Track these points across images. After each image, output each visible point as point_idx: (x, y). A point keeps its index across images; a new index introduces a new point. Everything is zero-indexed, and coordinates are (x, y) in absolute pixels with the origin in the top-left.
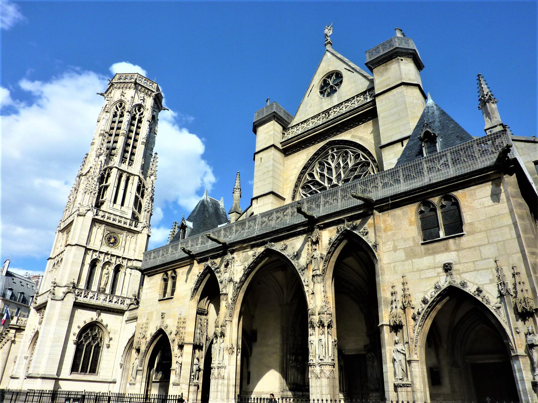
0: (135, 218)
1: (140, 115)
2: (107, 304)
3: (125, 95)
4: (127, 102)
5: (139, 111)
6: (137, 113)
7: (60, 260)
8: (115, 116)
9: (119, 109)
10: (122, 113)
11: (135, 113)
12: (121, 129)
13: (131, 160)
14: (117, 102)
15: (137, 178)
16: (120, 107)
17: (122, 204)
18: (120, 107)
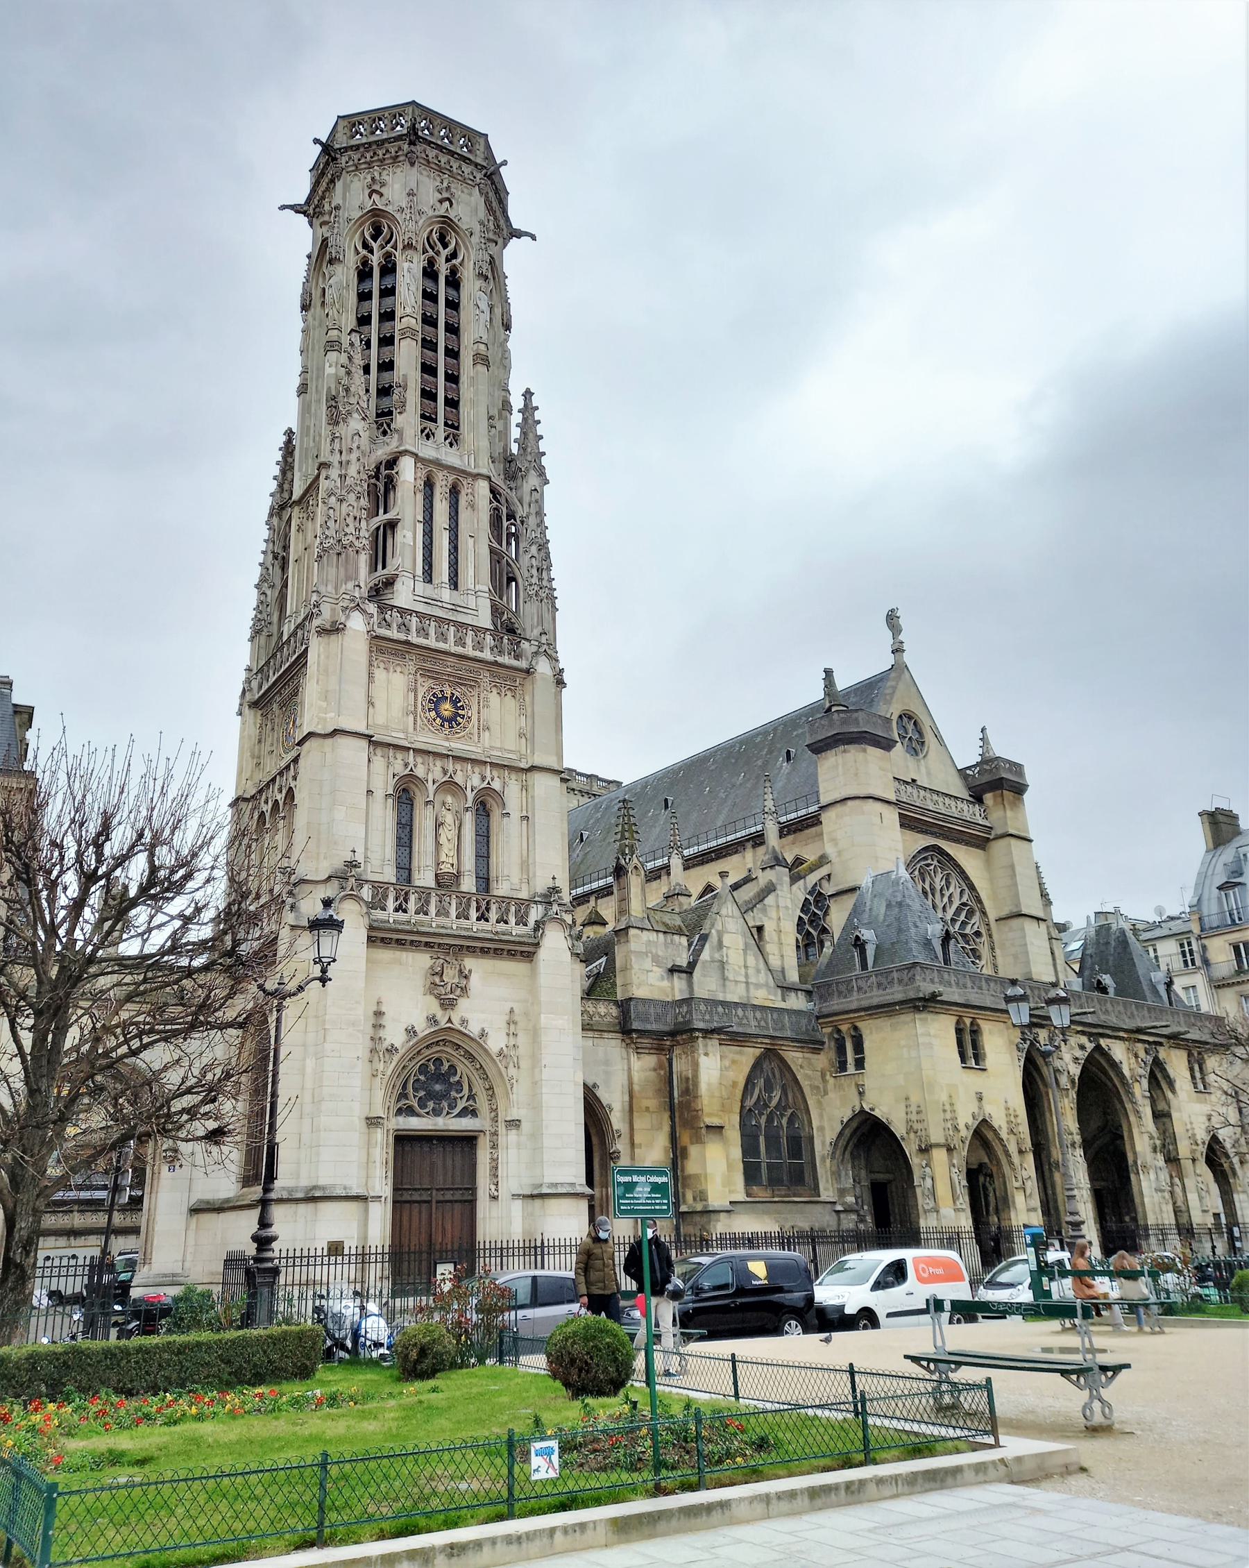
0: (507, 629)
1: (447, 260)
2: (473, 925)
3: (382, 190)
4: (397, 216)
5: (445, 246)
6: (438, 253)
7: (280, 797)
8: (364, 273)
9: (375, 246)
10: (388, 256)
11: (431, 253)
12: (398, 315)
13: (453, 426)
14: (360, 222)
15: (483, 488)
16: (375, 238)
17: (454, 583)
18: (375, 238)
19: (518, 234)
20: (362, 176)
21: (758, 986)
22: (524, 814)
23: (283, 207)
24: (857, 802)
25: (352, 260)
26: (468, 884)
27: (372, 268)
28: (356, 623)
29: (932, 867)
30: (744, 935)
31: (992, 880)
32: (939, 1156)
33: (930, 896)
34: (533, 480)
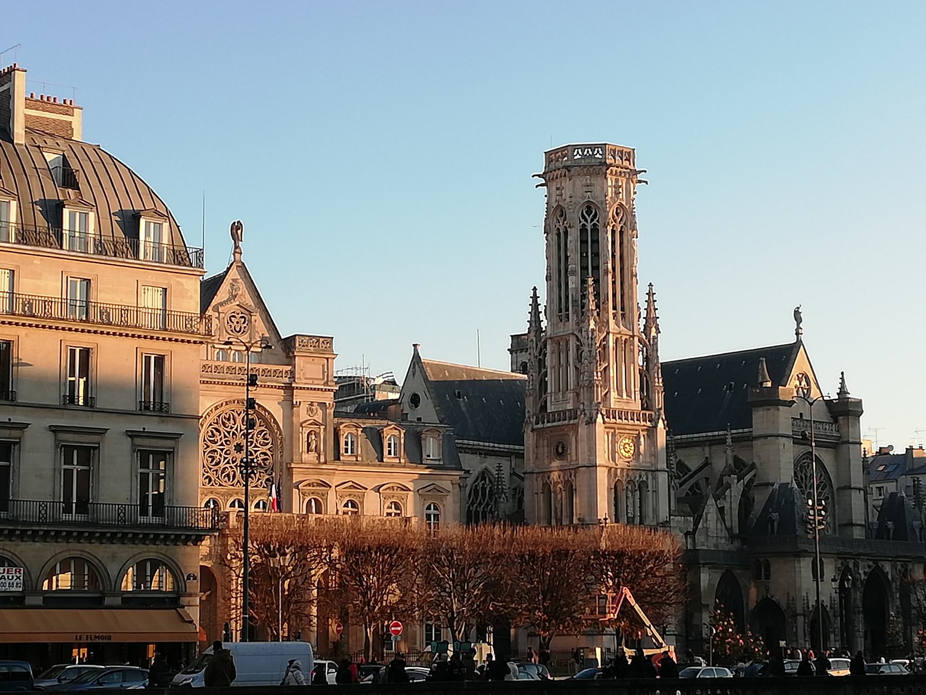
8: (583, 230)
19: (640, 182)
20: (581, 179)
21: (721, 538)
22: (654, 490)
23: (533, 176)
24: (772, 438)
25: (579, 226)
26: (637, 520)
27: (587, 230)
28: (599, 419)
29: (806, 464)
30: (717, 514)
31: (837, 466)
32: (800, 619)
33: (804, 480)
34: (653, 334)
